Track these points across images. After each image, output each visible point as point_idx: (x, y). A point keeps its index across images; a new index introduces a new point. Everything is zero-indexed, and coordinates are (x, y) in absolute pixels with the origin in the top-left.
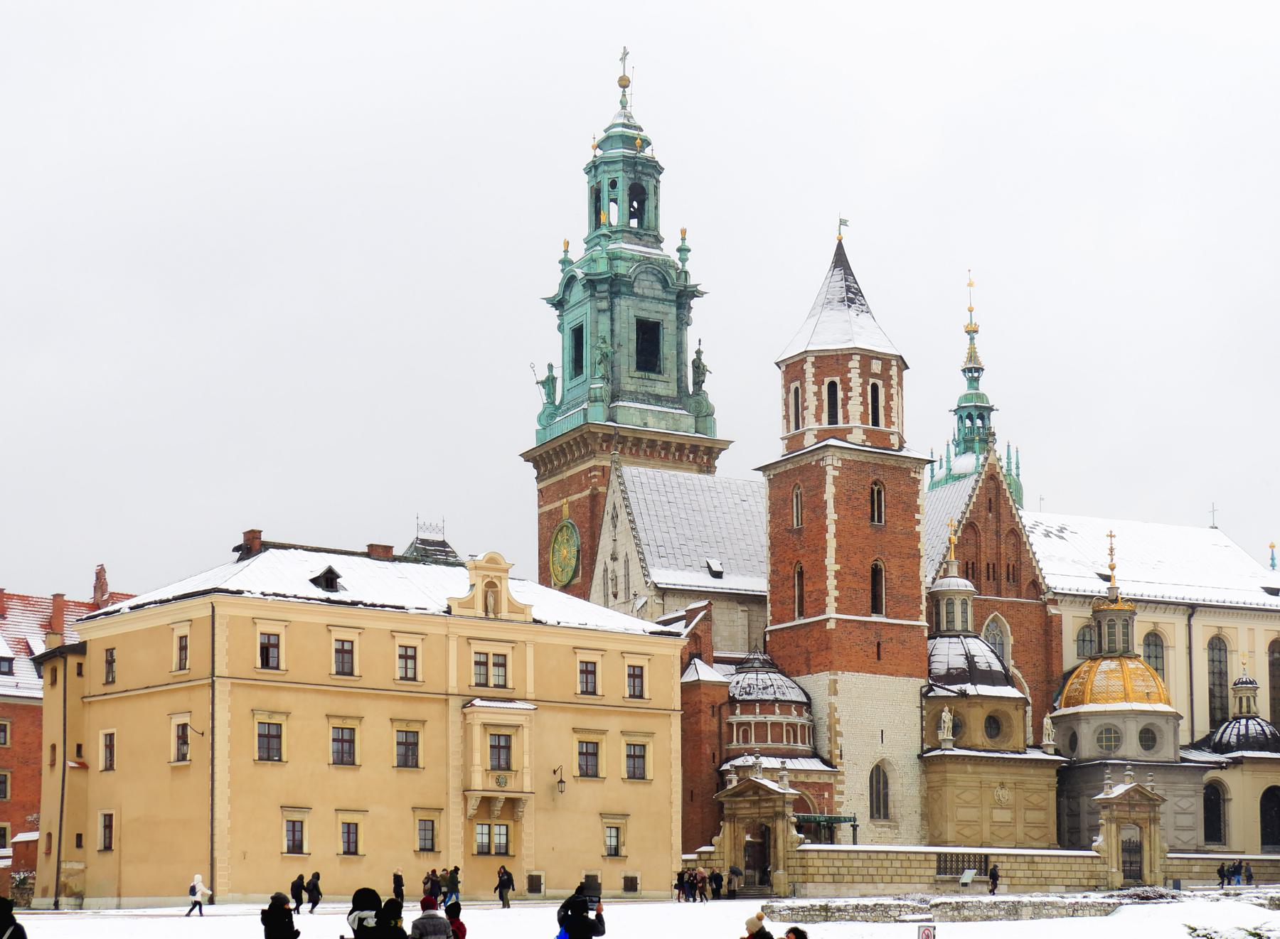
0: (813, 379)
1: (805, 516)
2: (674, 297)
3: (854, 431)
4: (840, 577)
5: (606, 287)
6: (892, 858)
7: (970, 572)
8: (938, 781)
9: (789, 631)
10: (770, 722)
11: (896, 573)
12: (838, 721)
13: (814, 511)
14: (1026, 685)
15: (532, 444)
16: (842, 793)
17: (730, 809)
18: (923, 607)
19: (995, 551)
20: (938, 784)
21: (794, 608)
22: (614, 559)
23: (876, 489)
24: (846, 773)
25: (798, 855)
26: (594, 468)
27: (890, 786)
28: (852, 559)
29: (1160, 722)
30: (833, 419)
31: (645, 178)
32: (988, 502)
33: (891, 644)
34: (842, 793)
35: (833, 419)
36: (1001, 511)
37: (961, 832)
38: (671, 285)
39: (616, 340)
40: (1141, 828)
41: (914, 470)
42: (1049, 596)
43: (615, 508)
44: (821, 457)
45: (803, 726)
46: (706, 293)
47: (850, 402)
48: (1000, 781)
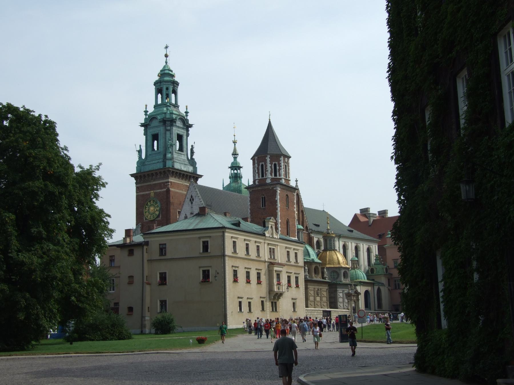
0: (269, 162)
1: (266, 204)
5: (169, 123)
15: (134, 171)
18: (296, 234)
26: (168, 182)
29: (347, 271)
30: (276, 175)
31: (176, 88)
35: (276, 175)
42: (310, 231)
43: (192, 197)
44: (274, 186)
47: (281, 170)
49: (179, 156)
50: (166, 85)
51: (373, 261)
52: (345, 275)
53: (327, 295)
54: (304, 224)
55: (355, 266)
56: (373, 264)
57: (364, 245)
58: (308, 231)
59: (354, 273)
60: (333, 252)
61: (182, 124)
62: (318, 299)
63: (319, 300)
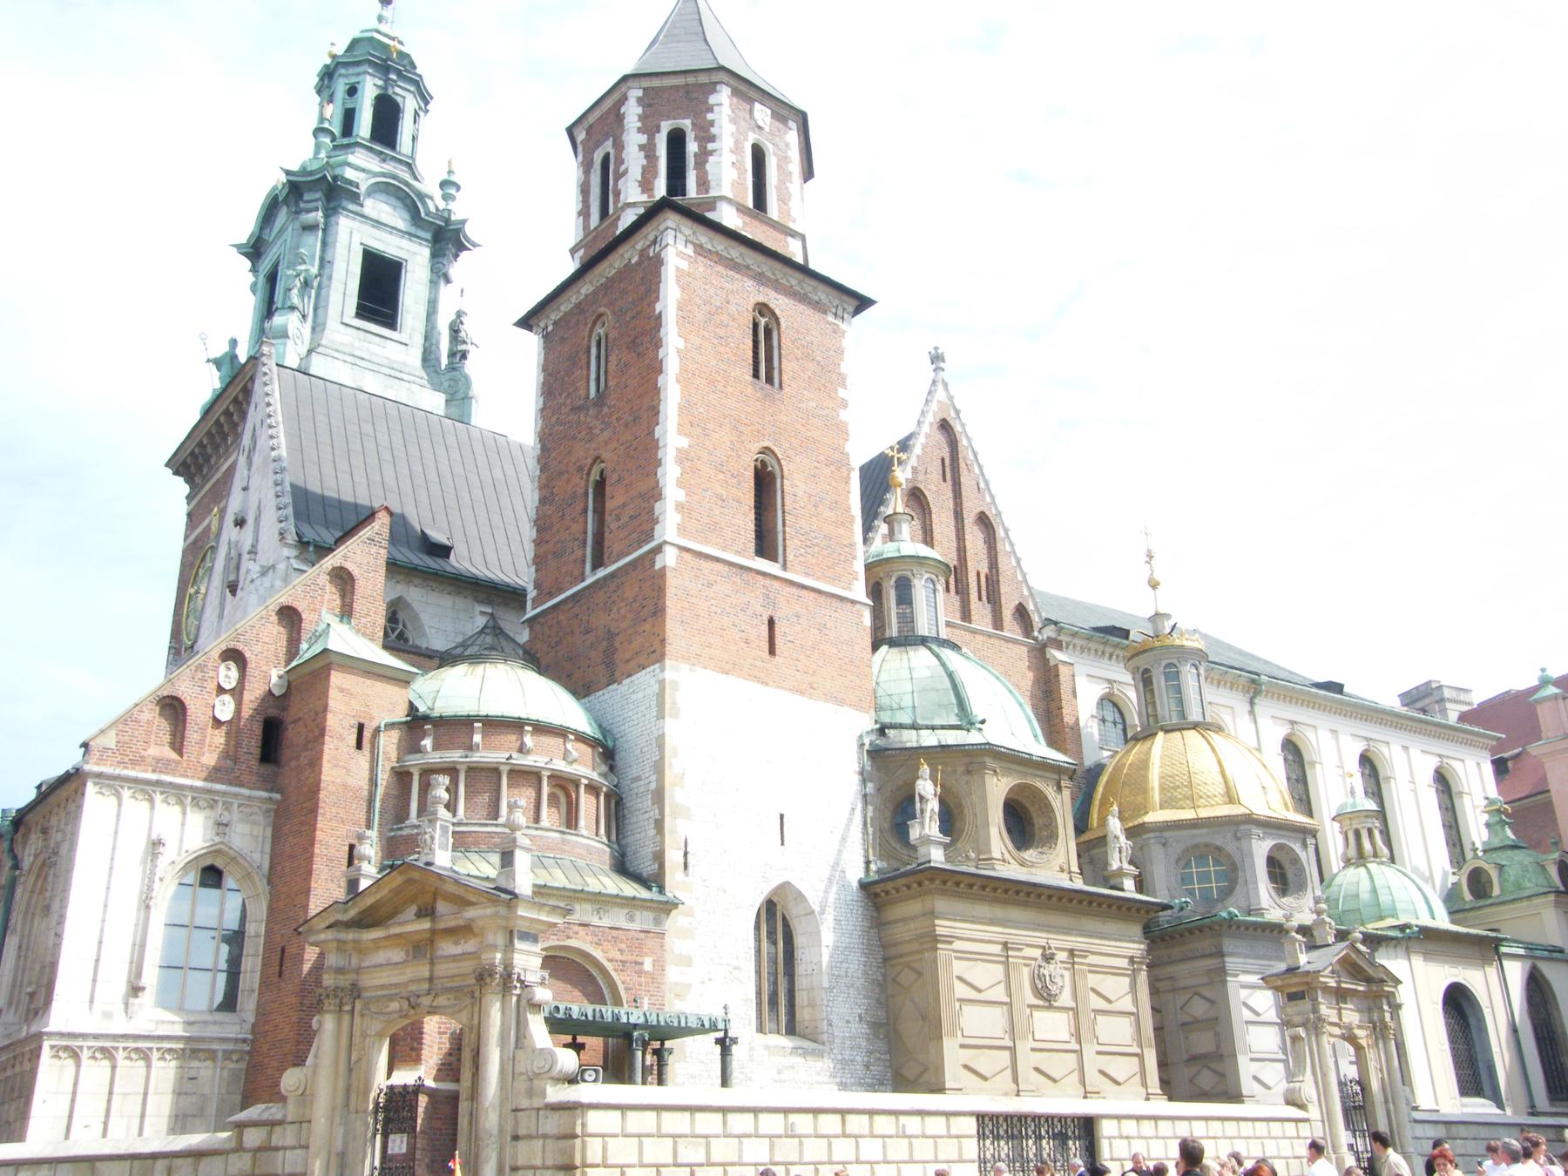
0: (639, 124)
2: (428, 236)
3: (718, 204)
5: (318, 195)
6: (856, 1131)
8: (910, 941)
9: (570, 605)
10: (508, 768)
13: (633, 345)
16: (687, 961)
17: (339, 971)
18: (859, 567)
19: (954, 544)
20: (916, 946)
21: (584, 556)
22: (240, 523)
25: (551, 1124)
27: (798, 953)
29: (1297, 847)
31: (397, 90)
33: (798, 628)
34: (687, 961)
36: (962, 480)
38: (423, 215)
39: (327, 271)
40: (1359, 1048)
42: (1049, 632)
44: (651, 237)
45: (593, 789)
46: (479, 245)
48: (1043, 942)
49: (366, 345)
50: (346, 76)
51: (1477, 831)
52: (1283, 875)
53: (1135, 1001)
54: (1003, 589)
55: (1367, 846)
56: (1479, 845)
57: (1415, 752)
58: (1036, 634)
59: (1365, 886)
60: (1191, 736)
61: (406, 216)
62: (1052, 1026)
63: (1066, 1037)
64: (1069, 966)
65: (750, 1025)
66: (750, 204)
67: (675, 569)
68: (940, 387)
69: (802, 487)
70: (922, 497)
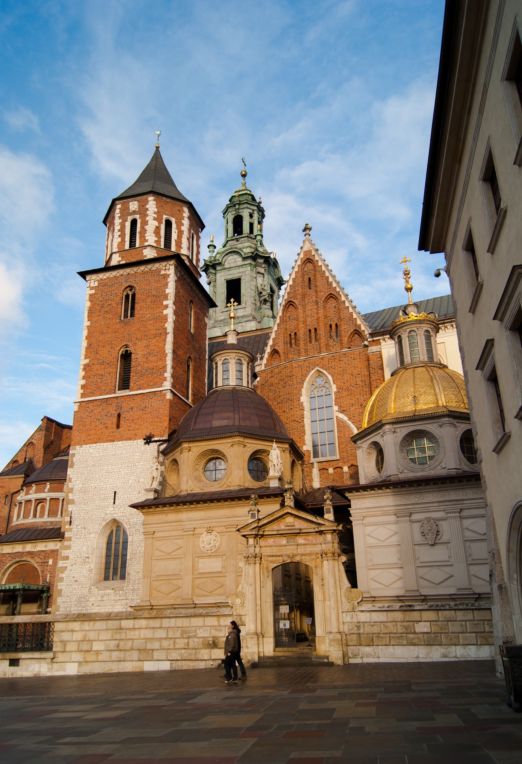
4: (88, 369)
7: (293, 341)
11: (141, 353)
12: (71, 490)
14: (352, 426)
16: (67, 558)
18: (168, 375)
23: (130, 293)
24: (73, 537)
28: (101, 352)
31: (240, 211)
32: (307, 281)
33: (131, 413)
34: (67, 558)
37: (157, 589)
41: (164, 268)
42: (369, 340)
48: (206, 525)
64: (226, 534)
65: (90, 579)
66: (127, 247)
67: (77, 411)
68: (307, 243)
69: (141, 353)
70: (294, 304)
